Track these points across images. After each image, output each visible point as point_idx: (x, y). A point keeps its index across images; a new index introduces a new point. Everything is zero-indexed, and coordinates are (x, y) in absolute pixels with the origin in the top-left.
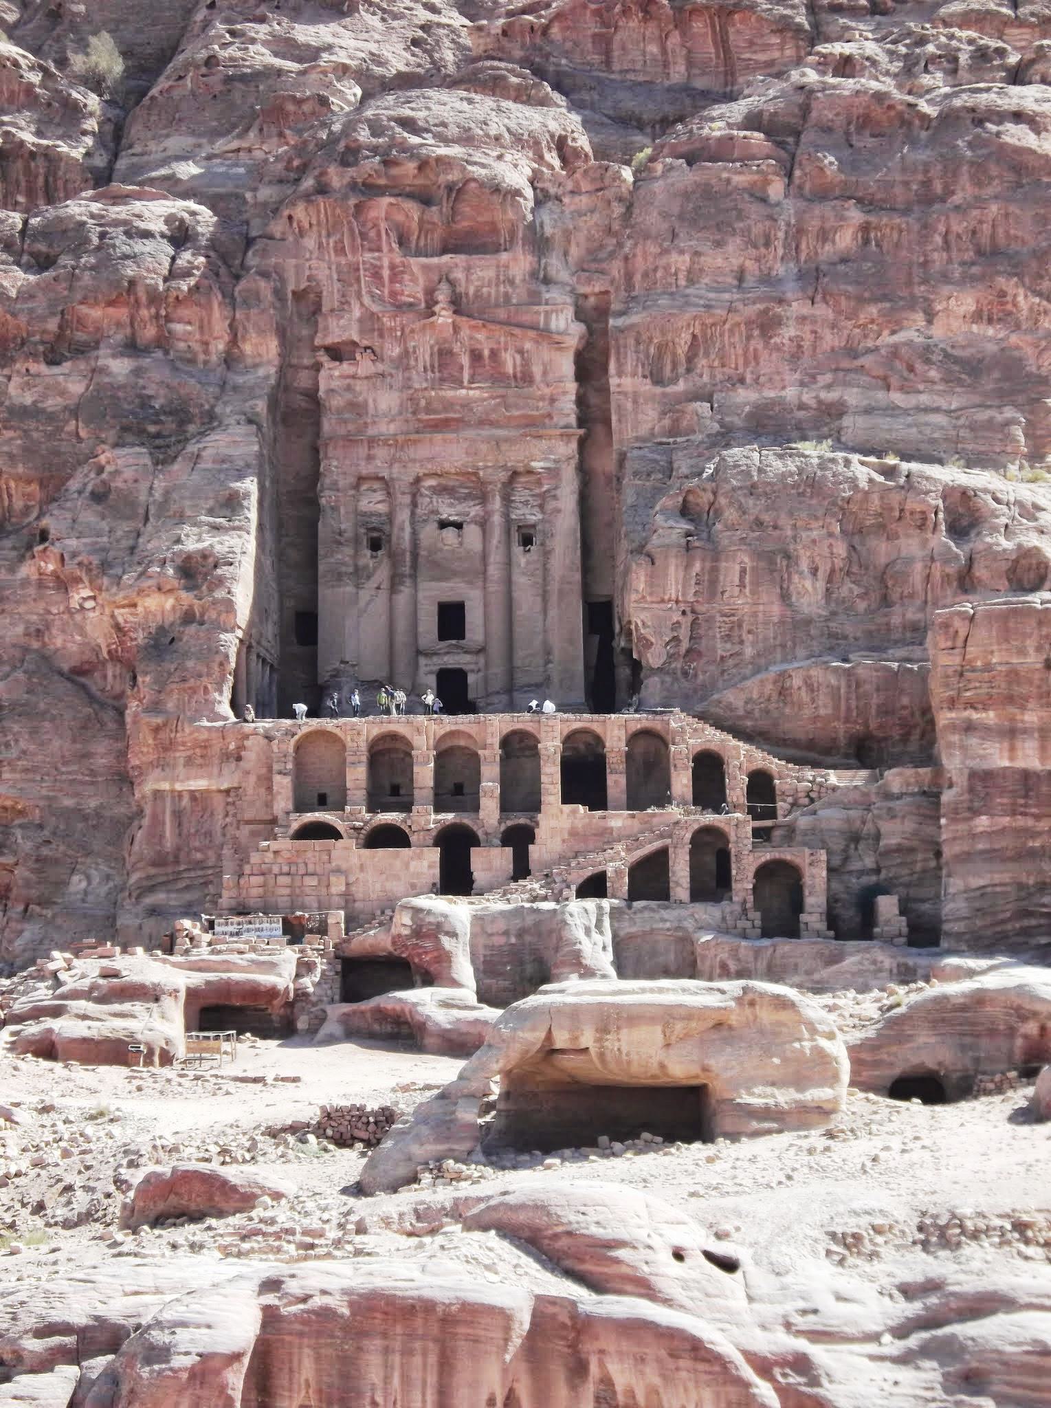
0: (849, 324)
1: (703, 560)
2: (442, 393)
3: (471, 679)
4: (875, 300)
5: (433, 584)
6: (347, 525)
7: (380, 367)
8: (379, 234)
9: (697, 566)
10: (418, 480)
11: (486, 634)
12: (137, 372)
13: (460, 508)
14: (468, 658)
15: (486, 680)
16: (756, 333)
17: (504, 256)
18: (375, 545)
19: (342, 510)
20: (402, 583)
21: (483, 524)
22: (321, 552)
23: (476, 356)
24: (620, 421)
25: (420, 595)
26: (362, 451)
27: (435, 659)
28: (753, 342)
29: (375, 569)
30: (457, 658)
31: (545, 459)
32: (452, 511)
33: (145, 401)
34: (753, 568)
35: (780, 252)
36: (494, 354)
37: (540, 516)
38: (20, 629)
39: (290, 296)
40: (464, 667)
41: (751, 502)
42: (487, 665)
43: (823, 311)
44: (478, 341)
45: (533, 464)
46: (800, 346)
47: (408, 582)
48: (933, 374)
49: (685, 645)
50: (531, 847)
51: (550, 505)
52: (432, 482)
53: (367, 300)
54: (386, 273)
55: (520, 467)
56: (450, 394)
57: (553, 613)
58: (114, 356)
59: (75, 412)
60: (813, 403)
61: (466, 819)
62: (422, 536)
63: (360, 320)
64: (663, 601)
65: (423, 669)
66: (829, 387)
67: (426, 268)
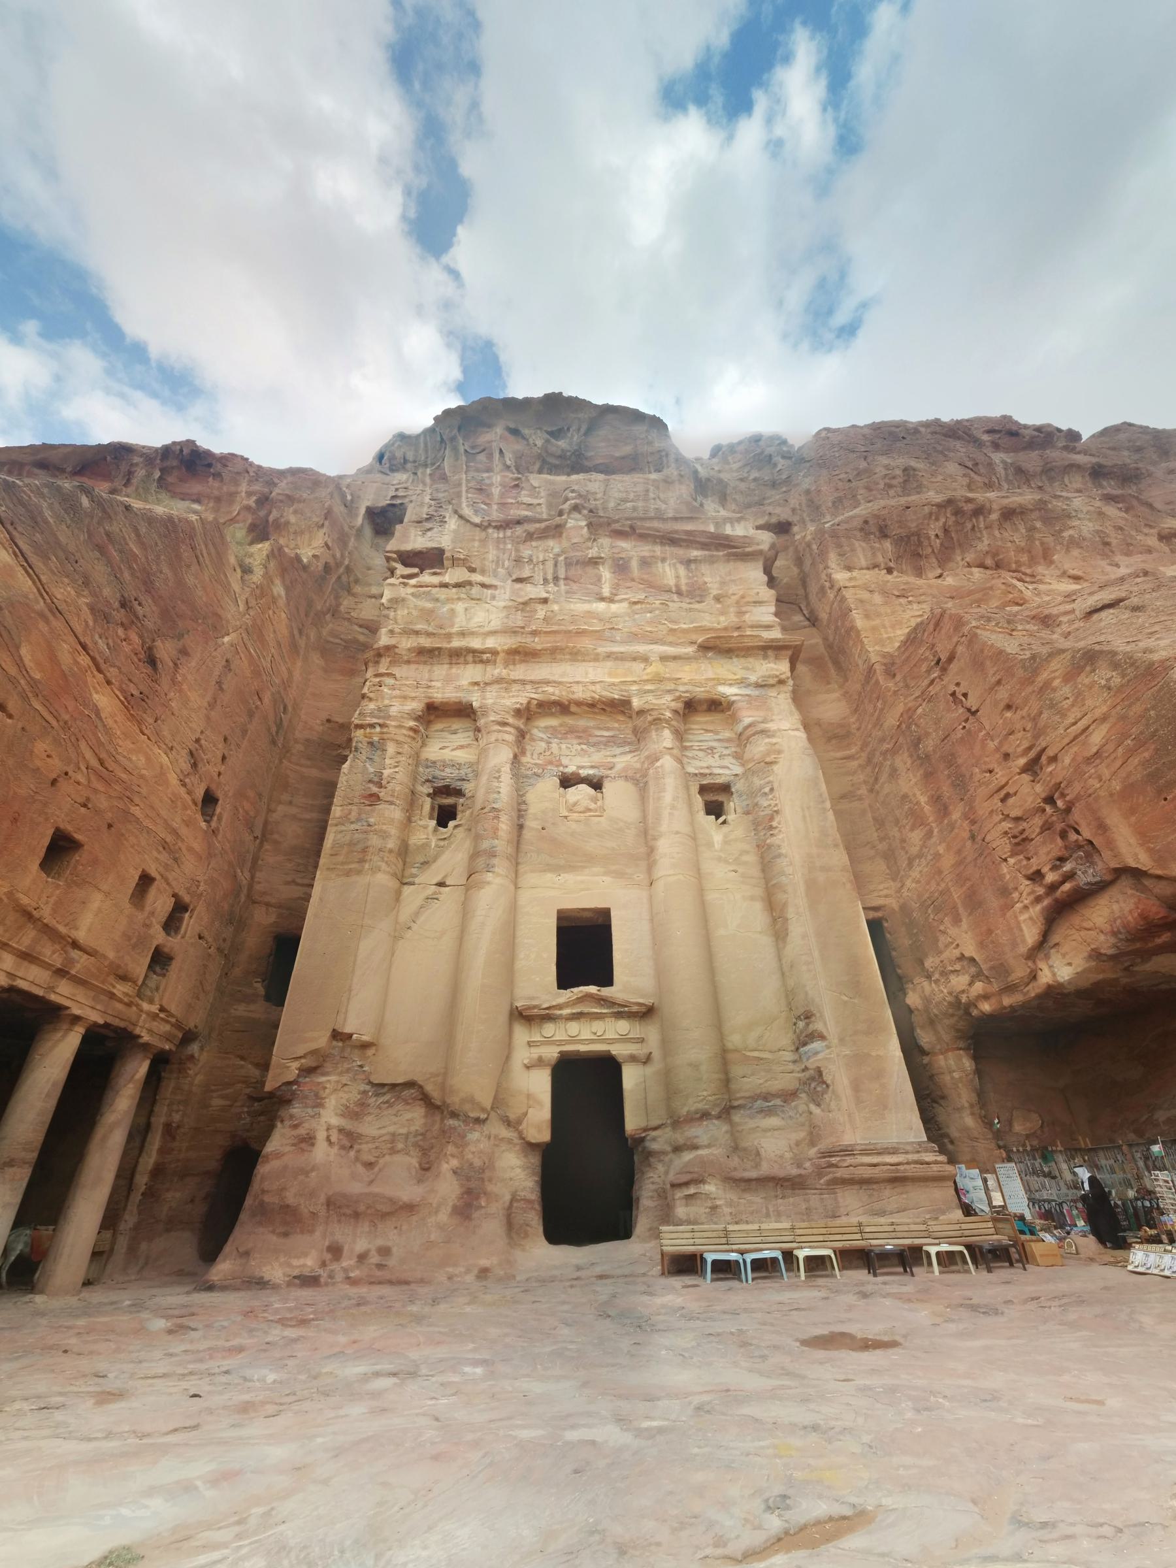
2: (572, 606)
3: (630, 1078)
5: (549, 876)
6: (395, 768)
7: (477, 578)
8: (490, 456)
10: (527, 713)
11: (661, 972)
13: (598, 757)
14: (623, 1026)
15: (667, 1078)
16: (1038, 525)
18: (445, 816)
19: (391, 748)
20: (489, 868)
22: (336, 811)
23: (621, 567)
24: (867, 617)
25: (524, 897)
26: (441, 670)
27: (549, 1029)
28: (1037, 535)
29: (441, 850)
30: (598, 1027)
31: (742, 682)
32: (585, 761)
36: (645, 563)
37: (738, 770)
39: (363, 511)
40: (617, 1050)
42: (666, 1044)
44: (623, 550)
45: (723, 689)
47: (501, 866)
51: (758, 748)
52: (553, 722)
55: (700, 692)
56: (586, 607)
57: (800, 926)
62: (531, 797)
63: (455, 531)
65: (522, 1054)
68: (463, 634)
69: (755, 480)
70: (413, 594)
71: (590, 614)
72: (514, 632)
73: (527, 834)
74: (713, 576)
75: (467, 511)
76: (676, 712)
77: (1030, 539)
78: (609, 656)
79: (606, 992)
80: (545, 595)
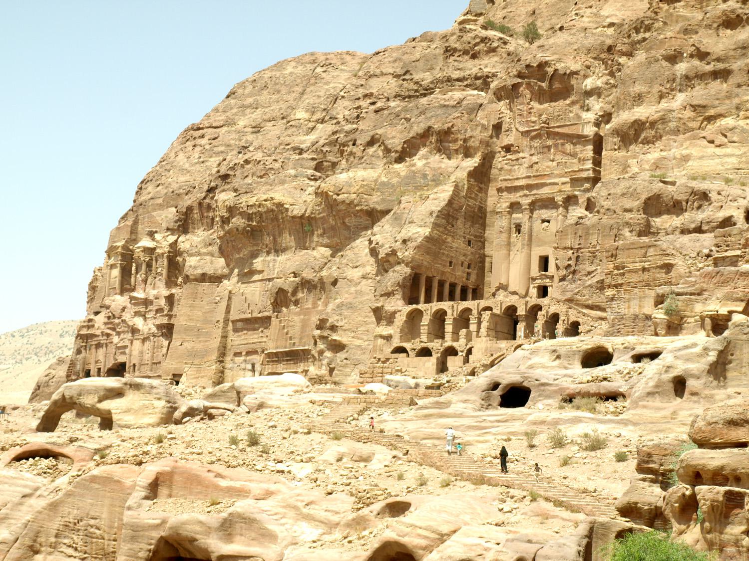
0: (701, 118)
1: (583, 229)
4: (714, 107)
7: (521, 155)
9: (580, 233)
12: (425, 165)
17: (568, 101)
19: (504, 217)
21: (556, 220)
23: (556, 146)
25: (532, 253)
31: (580, 191)
33: (425, 176)
34: (602, 232)
35: (678, 88)
38: (360, 274)
39: (491, 127)
41: (606, 203)
43: (689, 113)
46: (679, 131)
47: (526, 247)
48: (735, 139)
49: (572, 268)
50: (470, 356)
52: (540, 204)
53: (518, 126)
54: (525, 113)
58: (419, 159)
59: (400, 184)
60: (678, 156)
61: (455, 345)
64: (565, 248)
66: (687, 148)
67: (539, 110)
68: (517, 179)
69: (610, 83)
70: (506, 164)
71: (548, 167)
72: (529, 177)
73: (533, 238)
74: (579, 148)
75: (518, 126)
76: (563, 202)
77: (656, 132)
78: (551, 184)
79: (547, 273)
80: (537, 160)
